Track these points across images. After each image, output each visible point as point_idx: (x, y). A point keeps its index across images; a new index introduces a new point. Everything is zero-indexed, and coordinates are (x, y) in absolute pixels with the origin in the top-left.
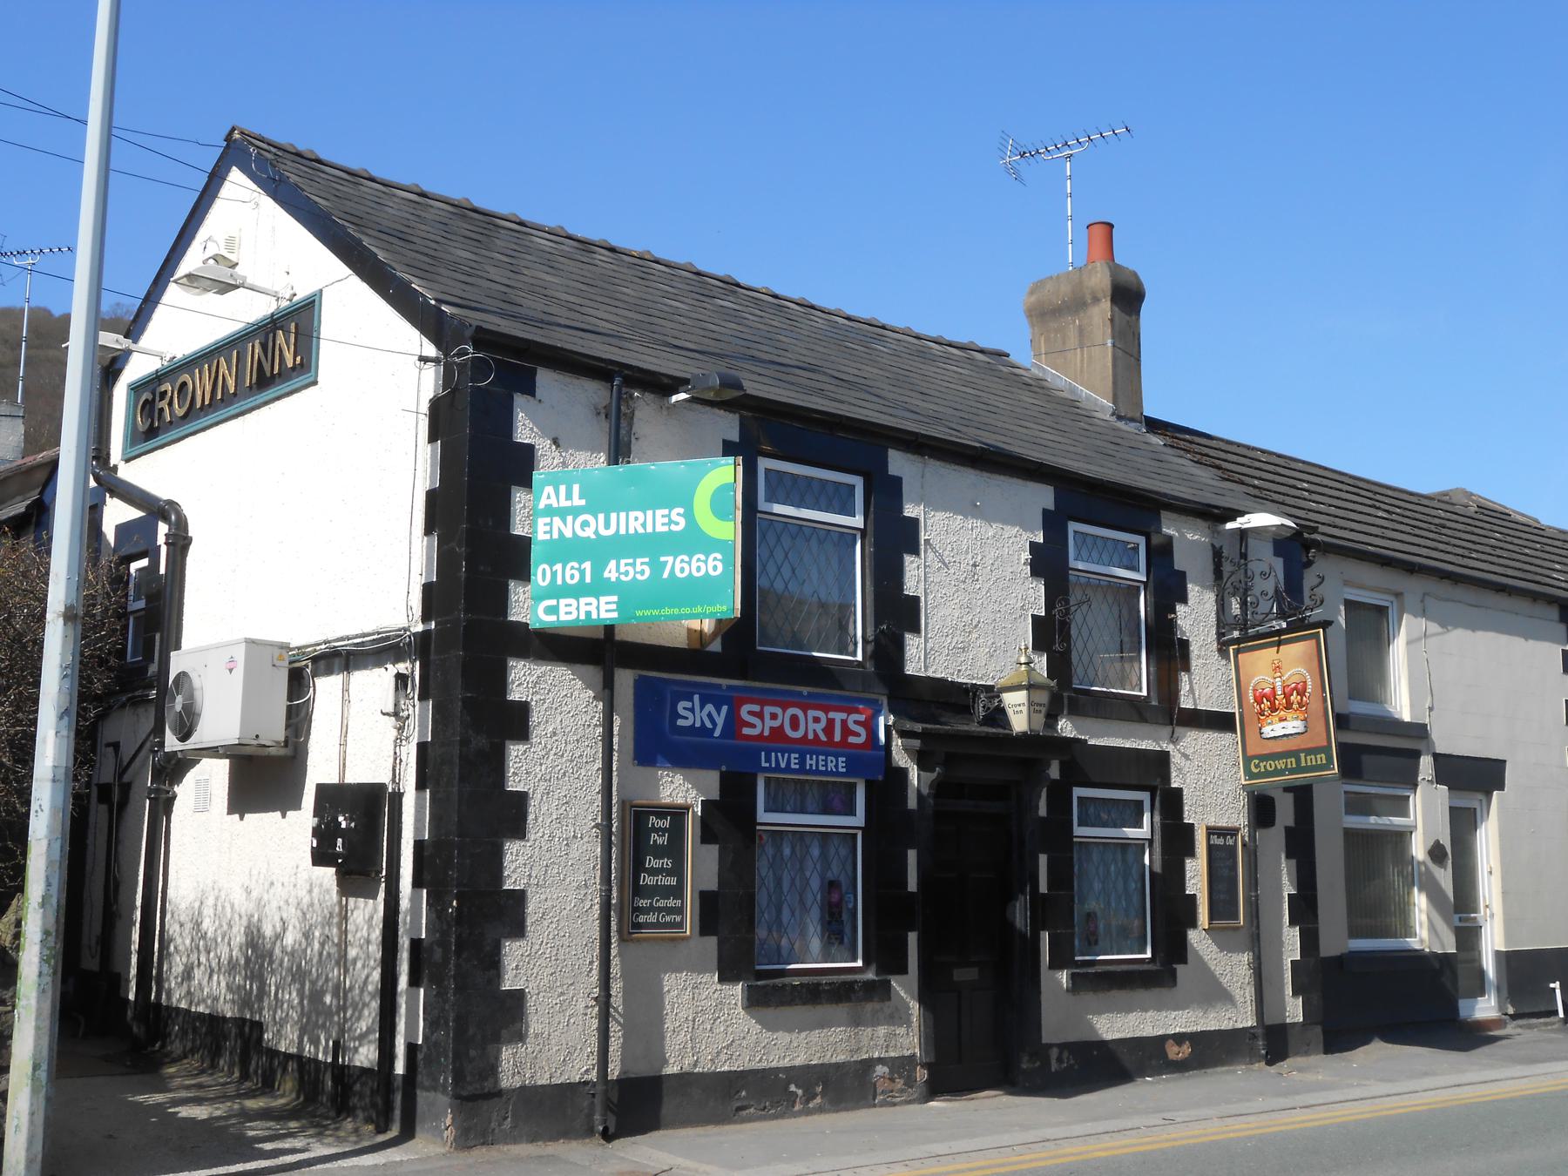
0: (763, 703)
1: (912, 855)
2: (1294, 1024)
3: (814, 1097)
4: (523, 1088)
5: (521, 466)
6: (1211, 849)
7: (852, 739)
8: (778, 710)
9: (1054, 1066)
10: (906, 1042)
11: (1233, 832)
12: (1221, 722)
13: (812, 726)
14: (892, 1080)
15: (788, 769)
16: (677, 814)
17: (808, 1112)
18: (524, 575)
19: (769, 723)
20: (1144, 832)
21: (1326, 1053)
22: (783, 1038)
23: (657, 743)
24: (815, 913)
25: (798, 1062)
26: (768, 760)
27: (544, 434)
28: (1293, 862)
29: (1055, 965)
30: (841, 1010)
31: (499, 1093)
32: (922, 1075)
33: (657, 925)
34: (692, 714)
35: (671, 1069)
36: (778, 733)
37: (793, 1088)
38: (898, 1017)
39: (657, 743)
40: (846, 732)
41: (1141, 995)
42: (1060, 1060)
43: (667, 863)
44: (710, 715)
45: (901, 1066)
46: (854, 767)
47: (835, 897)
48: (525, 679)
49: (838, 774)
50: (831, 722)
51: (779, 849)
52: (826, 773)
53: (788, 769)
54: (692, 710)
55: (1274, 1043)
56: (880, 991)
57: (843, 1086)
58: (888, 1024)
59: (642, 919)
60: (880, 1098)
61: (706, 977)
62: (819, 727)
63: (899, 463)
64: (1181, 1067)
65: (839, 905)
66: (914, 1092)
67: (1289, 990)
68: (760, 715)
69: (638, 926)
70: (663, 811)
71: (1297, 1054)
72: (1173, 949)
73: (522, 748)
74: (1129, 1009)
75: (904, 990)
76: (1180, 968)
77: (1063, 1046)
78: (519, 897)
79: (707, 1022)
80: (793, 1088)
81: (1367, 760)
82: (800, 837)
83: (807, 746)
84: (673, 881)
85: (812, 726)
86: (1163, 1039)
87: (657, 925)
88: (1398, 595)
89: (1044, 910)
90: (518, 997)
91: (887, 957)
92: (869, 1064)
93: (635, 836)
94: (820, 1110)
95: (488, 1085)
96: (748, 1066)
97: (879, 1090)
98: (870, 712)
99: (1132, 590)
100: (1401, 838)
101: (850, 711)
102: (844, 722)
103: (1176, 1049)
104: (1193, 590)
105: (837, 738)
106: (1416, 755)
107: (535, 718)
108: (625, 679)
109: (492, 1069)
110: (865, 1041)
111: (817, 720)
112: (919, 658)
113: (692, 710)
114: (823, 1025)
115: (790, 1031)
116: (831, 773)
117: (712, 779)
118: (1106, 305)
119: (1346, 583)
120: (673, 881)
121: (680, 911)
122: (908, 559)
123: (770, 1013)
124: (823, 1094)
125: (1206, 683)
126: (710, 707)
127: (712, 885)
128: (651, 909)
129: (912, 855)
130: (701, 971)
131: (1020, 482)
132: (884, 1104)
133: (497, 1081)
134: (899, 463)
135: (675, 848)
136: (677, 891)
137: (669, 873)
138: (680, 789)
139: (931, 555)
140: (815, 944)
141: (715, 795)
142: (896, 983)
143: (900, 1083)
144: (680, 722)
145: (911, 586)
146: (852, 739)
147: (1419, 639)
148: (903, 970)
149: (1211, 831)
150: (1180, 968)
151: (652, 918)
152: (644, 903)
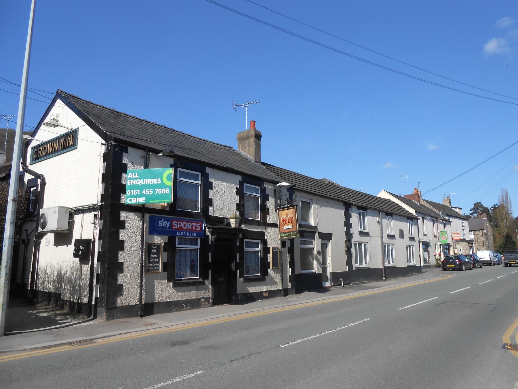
0: (178, 222)
1: (210, 254)
4: (122, 306)
5: (124, 168)
6: (273, 252)
9: (240, 298)
10: (208, 294)
11: (278, 248)
12: (275, 226)
13: (188, 226)
15: (183, 235)
16: (158, 245)
17: (186, 310)
18: (124, 192)
19: (179, 226)
20: (259, 249)
21: (296, 294)
22: (181, 294)
23: (154, 230)
24: (189, 266)
25: (184, 299)
27: (130, 162)
29: (240, 277)
31: (117, 307)
32: (211, 301)
33: (153, 270)
34: (162, 223)
35: (156, 301)
36: (181, 228)
38: (206, 289)
39: (154, 230)
40: (196, 227)
41: (258, 283)
43: (156, 256)
46: (197, 236)
47: (193, 263)
48: (124, 216)
50: (193, 225)
51: (181, 253)
52: (191, 236)
53: (183, 235)
55: (285, 292)
56: (202, 283)
57: (194, 304)
59: (150, 268)
61: (164, 281)
62: (190, 226)
63: (208, 170)
64: (266, 298)
65: (194, 265)
66: (210, 305)
67: (289, 281)
69: (149, 270)
70: (155, 245)
72: (265, 273)
73: (123, 231)
75: (208, 283)
76: (266, 277)
77: (241, 294)
78: (122, 264)
79: (164, 290)
82: (186, 250)
83: (187, 230)
84: (157, 260)
85: (188, 226)
86: (263, 292)
87: (153, 270)
88: (312, 200)
89: (238, 266)
90: (121, 286)
91: (204, 276)
93: (149, 251)
94: (189, 309)
95: (114, 306)
99: (257, 198)
100: (312, 250)
102: (195, 226)
104: (270, 198)
106: (315, 232)
107: (126, 224)
108: (147, 216)
109: (115, 302)
111: (189, 225)
112: (212, 212)
114: (190, 291)
115: (183, 292)
117: (166, 238)
118: (254, 138)
119: (301, 197)
120: (157, 260)
121: (159, 266)
122: (210, 190)
124: (190, 305)
125: (272, 218)
126: (166, 222)
127: (166, 261)
128: (152, 266)
129: (210, 254)
130: (163, 279)
132: (203, 307)
133: (116, 305)
134: (208, 170)
135: (158, 253)
136: (158, 262)
137: (156, 258)
138: (159, 240)
140: (189, 273)
141: (167, 241)
145: (211, 196)
149: (273, 248)
151: (152, 268)
152: (150, 265)
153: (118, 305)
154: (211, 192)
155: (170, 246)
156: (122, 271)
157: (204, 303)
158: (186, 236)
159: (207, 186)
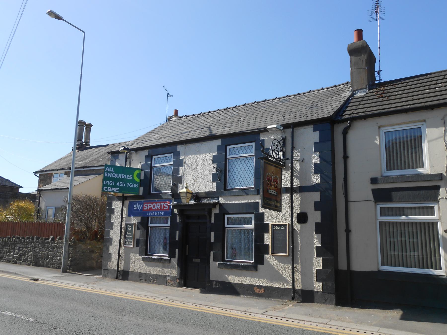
1: (177, 232)
2: (318, 292)
6: (273, 231)
7: (165, 208)
8: (151, 204)
11: (284, 225)
13: (157, 206)
17: (153, 283)
19: (149, 207)
22: (150, 268)
23: (131, 213)
25: (152, 273)
28: (320, 235)
29: (215, 260)
30: (161, 264)
31: (107, 269)
35: (130, 270)
38: (173, 267)
39: (131, 213)
40: (164, 207)
41: (245, 272)
42: (216, 285)
43: (130, 233)
45: (173, 278)
50: (161, 205)
52: (159, 216)
55: (306, 297)
62: (159, 207)
64: (259, 296)
67: (315, 279)
68: (147, 206)
69: (125, 244)
70: (130, 225)
71: (318, 302)
75: (175, 261)
76: (260, 266)
77: (217, 282)
79: (137, 263)
81: (394, 194)
83: (157, 210)
84: (131, 237)
85: (157, 206)
86: (253, 286)
91: (172, 255)
92: (165, 276)
93: (125, 229)
94: (156, 283)
96: (143, 272)
101: (165, 203)
102: (163, 205)
103: (258, 290)
110: (165, 271)
111: (158, 205)
116: (161, 216)
117: (139, 218)
120: (131, 237)
123: (147, 262)
129: (177, 232)
134: (180, 148)
137: (131, 235)
138: (134, 221)
139: (186, 165)
142: (173, 260)
143: (172, 282)
145: (181, 174)
146: (165, 208)
147: (440, 137)
148: (174, 257)
149: (273, 226)
153: (108, 268)
154: (181, 169)
155: (144, 224)
156: (111, 244)
157: (170, 282)
158: (155, 215)
159: (179, 163)
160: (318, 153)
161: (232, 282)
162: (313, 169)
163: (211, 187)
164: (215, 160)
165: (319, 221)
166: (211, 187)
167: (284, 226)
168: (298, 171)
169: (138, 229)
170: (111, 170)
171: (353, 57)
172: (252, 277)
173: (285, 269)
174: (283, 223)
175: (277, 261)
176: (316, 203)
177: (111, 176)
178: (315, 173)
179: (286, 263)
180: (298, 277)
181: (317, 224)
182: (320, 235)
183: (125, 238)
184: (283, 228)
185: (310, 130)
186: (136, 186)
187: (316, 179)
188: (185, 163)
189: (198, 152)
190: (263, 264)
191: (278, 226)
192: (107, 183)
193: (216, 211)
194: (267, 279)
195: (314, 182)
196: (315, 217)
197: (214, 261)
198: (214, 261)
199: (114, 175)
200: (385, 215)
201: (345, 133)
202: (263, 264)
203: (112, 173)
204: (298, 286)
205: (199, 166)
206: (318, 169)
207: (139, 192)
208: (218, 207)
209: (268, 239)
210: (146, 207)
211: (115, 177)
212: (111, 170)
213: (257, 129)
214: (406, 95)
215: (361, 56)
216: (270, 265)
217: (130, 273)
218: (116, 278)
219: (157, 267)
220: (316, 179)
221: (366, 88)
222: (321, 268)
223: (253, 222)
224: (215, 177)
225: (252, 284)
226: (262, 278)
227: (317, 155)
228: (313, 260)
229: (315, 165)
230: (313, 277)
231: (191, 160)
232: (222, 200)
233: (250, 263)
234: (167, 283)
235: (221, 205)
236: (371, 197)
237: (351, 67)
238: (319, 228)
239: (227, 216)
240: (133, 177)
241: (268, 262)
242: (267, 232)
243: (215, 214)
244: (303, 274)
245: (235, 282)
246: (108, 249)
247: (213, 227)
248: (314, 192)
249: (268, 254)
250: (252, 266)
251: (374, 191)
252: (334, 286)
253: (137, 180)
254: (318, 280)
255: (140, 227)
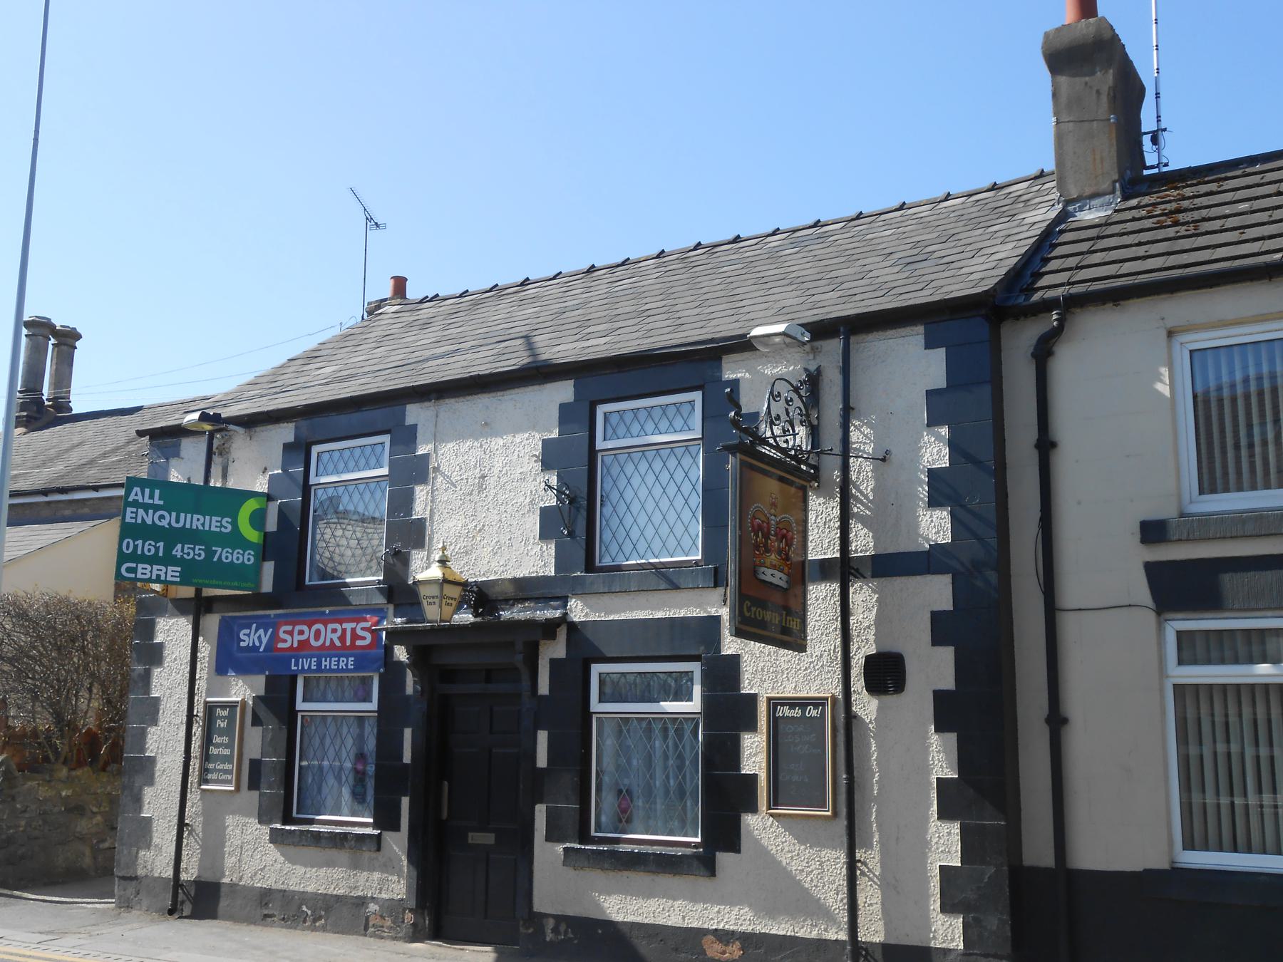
1: (408, 733)
2: (946, 951)
3: (320, 918)
6: (775, 724)
7: (359, 643)
8: (305, 628)
9: (549, 936)
11: (818, 702)
13: (330, 635)
14: (382, 917)
17: (314, 929)
19: (297, 638)
22: (300, 870)
23: (228, 661)
26: (297, 664)
28: (952, 737)
29: (551, 837)
30: (343, 855)
32: (409, 917)
35: (226, 880)
36: (304, 644)
37: (304, 908)
38: (389, 867)
39: (228, 661)
40: (355, 636)
41: (666, 880)
42: (555, 930)
43: (225, 739)
44: (259, 638)
45: (392, 908)
47: (360, 767)
49: (351, 671)
50: (344, 631)
51: (338, 730)
52: (338, 671)
54: (248, 635)
58: (383, 872)
60: (371, 930)
62: (335, 637)
66: (405, 929)
67: (935, 904)
68: (291, 633)
69: (207, 782)
70: (224, 706)
72: (723, 833)
74: (649, 895)
75: (397, 844)
76: (724, 859)
77: (559, 919)
79: (252, 853)
80: (304, 908)
83: (330, 650)
84: (228, 752)
85: (330, 635)
86: (701, 932)
91: (386, 819)
92: (362, 902)
93: (206, 723)
94: (324, 929)
97: (371, 924)
98: (376, 619)
101: (358, 621)
102: (353, 630)
103: (718, 947)
105: (348, 643)
110: (362, 882)
111: (334, 631)
113: (248, 635)
114: (330, 864)
115: (306, 866)
116: (342, 670)
117: (260, 681)
120: (228, 752)
123: (292, 850)
126: (261, 632)
128: (215, 770)
129: (408, 733)
130: (249, 815)
131: (536, 387)
133: (136, 870)
134: (415, 413)
137: (226, 746)
138: (241, 690)
141: (262, 692)
142: (389, 837)
143: (388, 922)
144: (242, 644)
145: (420, 510)
146: (359, 643)
148: (396, 828)
149: (774, 703)
150: (724, 859)
153: (141, 872)
154: (421, 493)
155: (278, 703)
157: (379, 922)
158: (319, 669)
159: (412, 471)
160: (944, 431)
161: (620, 918)
162: (923, 491)
163: (536, 559)
164: (550, 457)
165: (948, 683)
166: (536, 559)
167: (816, 706)
168: (866, 497)
169: (256, 721)
170: (151, 497)
171: (1063, 79)
172: (694, 900)
173: (819, 869)
174: (811, 694)
175: (789, 838)
176: (936, 617)
177: (149, 522)
178: (933, 503)
179: (823, 846)
180: (869, 896)
181: (939, 696)
182: (952, 737)
183: (206, 757)
184: (814, 713)
185: (911, 341)
186: (248, 558)
187: (935, 527)
188: (436, 469)
189: (488, 429)
190: (738, 851)
191: (792, 706)
192: (136, 547)
193: (556, 649)
194: (750, 906)
195: (927, 540)
196: (933, 669)
197: (549, 838)
198: (549, 838)
199: (162, 517)
200: (1195, 662)
201: (1043, 353)
202: (738, 851)
203: (156, 508)
204: (873, 932)
205: (491, 481)
206: (942, 489)
207: (258, 583)
208: (562, 634)
209: (754, 754)
210: (288, 637)
211: (164, 523)
212: (151, 497)
213: (712, 340)
214: (1263, 217)
215: (1093, 73)
216: (763, 853)
217: (223, 889)
218: (171, 912)
219: (329, 866)
220: (935, 527)
221: (1113, 192)
222: (957, 862)
223: (697, 690)
224: (550, 524)
225: (695, 925)
226: (732, 904)
227: (939, 438)
228: (926, 831)
229: (931, 473)
230: (927, 896)
231: (460, 459)
232: (578, 611)
233: (687, 845)
234: (366, 928)
235: (573, 628)
236: (1143, 593)
237: (1056, 114)
238: (947, 711)
239: (596, 669)
240: (234, 524)
241: (757, 842)
242: (752, 727)
243: (554, 663)
244: (889, 885)
245: (630, 919)
246: (138, 801)
247: (544, 713)
248: (929, 578)
249: (754, 809)
250: (695, 856)
251: (1154, 571)
252: (1008, 928)
253: (253, 536)
254: (946, 908)
255: (263, 713)
